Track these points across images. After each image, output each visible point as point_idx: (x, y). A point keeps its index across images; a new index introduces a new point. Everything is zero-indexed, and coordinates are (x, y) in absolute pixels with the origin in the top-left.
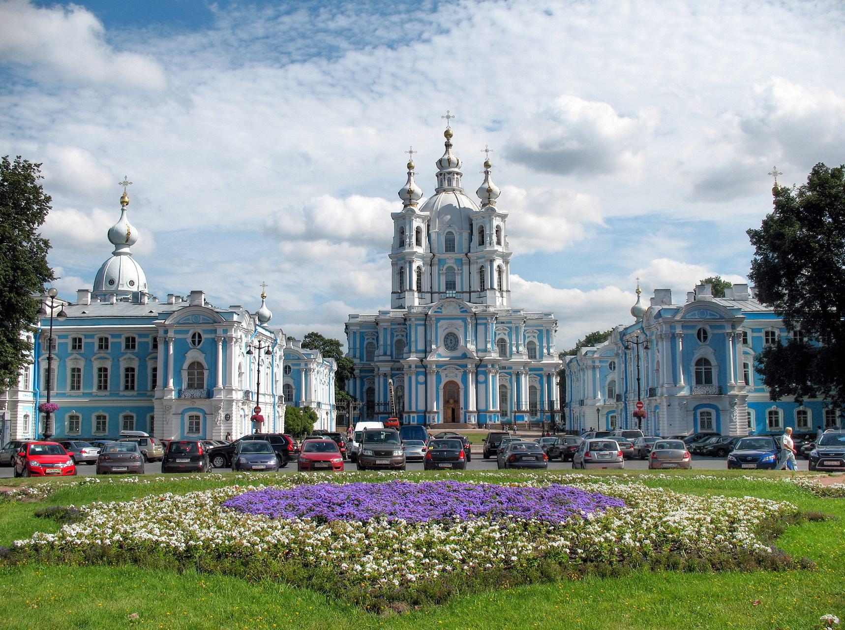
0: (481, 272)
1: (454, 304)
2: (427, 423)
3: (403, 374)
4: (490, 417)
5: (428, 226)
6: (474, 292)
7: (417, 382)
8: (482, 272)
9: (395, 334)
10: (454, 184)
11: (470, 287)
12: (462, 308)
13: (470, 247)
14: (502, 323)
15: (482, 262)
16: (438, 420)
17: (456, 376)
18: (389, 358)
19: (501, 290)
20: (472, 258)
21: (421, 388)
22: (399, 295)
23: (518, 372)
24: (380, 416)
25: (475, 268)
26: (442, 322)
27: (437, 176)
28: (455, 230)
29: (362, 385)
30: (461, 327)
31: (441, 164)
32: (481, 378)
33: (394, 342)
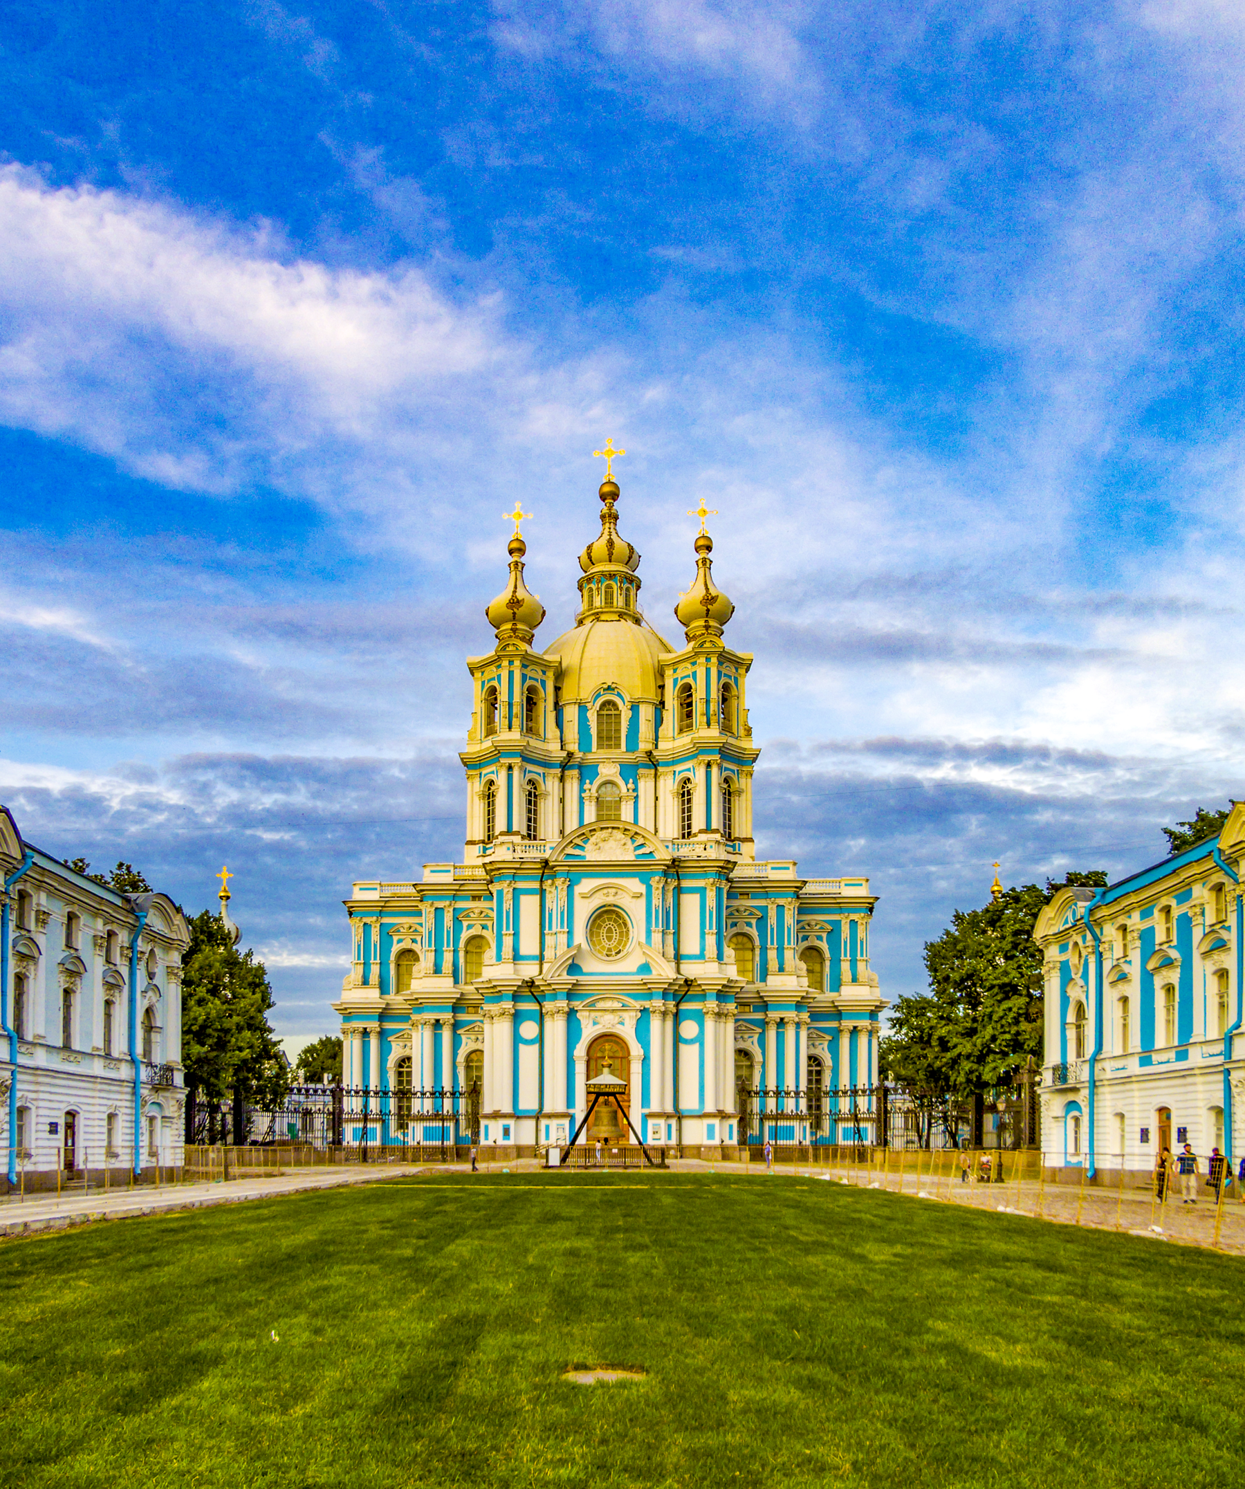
0: (683, 795)
1: (618, 835)
3: (482, 1022)
5: (557, 689)
7: (517, 1040)
9: (465, 924)
12: (642, 845)
13: (657, 739)
15: (689, 770)
17: (622, 1023)
21: (528, 1054)
22: (485, 849)
25: (669, 785)
26: (586, 885)
27: (581, 588)
28: (619, 695)
32: (689, 1029)
33: (462, 944)
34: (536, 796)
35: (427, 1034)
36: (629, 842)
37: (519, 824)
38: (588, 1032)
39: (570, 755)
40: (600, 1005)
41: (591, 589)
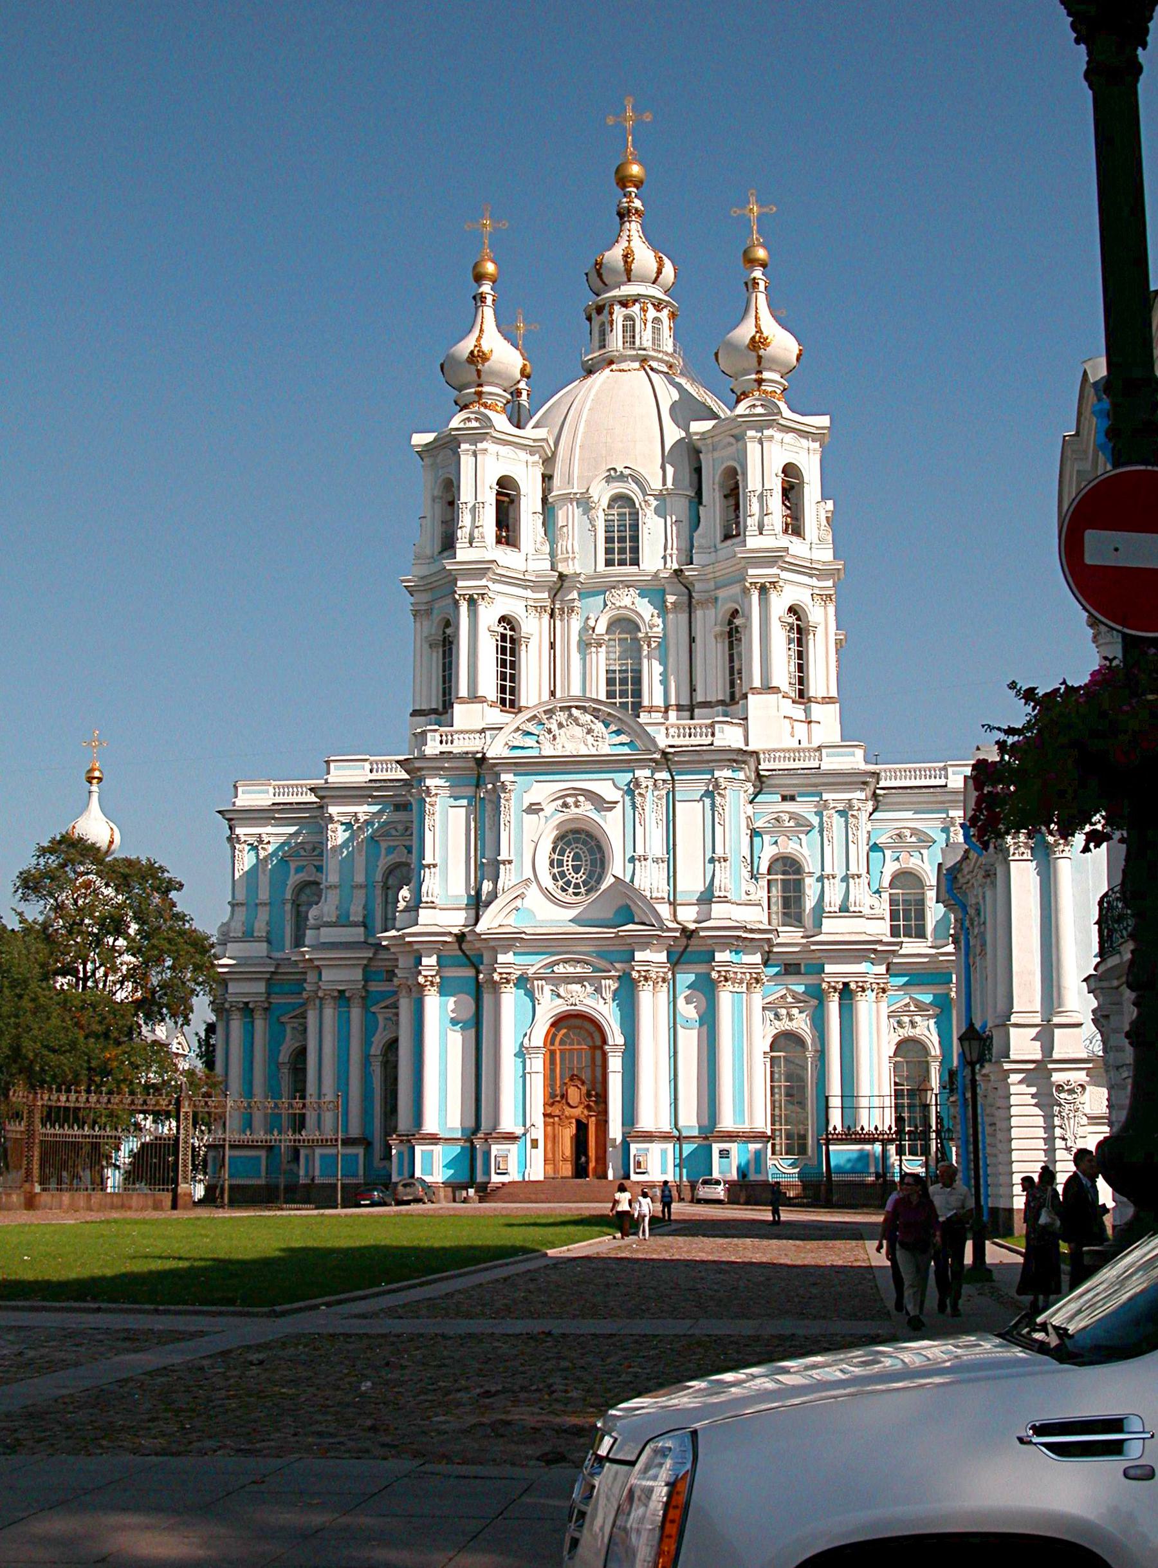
2: (480, 1178)
4: (724, 1154)
5: (547, 478)
6: (706, 704)
8: (733, 634)
10: (645, 338)
11: (693, 690)
14: (784, 798)
16: (524, 1164)
18: (358, 934)
19: (802, 696)
20: (698, 586)
23: (846, 985)
24: (318, 1151)
25: (709, 622)
26: (542, 790)
27: (589, 319)
29: (274, 1042)
30: (610, 806)
31: (600, 275)
33: (379, 877)
34: (513, 640)
35: (328, 1012)
36: (599, 727)
37: (488, 686)
38: (549, 1007)
39: (561, 576)
40: (559, 969)
41: (603, 324)
